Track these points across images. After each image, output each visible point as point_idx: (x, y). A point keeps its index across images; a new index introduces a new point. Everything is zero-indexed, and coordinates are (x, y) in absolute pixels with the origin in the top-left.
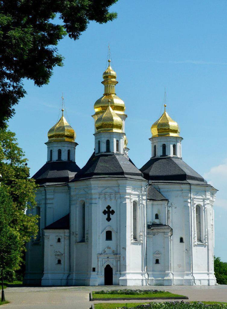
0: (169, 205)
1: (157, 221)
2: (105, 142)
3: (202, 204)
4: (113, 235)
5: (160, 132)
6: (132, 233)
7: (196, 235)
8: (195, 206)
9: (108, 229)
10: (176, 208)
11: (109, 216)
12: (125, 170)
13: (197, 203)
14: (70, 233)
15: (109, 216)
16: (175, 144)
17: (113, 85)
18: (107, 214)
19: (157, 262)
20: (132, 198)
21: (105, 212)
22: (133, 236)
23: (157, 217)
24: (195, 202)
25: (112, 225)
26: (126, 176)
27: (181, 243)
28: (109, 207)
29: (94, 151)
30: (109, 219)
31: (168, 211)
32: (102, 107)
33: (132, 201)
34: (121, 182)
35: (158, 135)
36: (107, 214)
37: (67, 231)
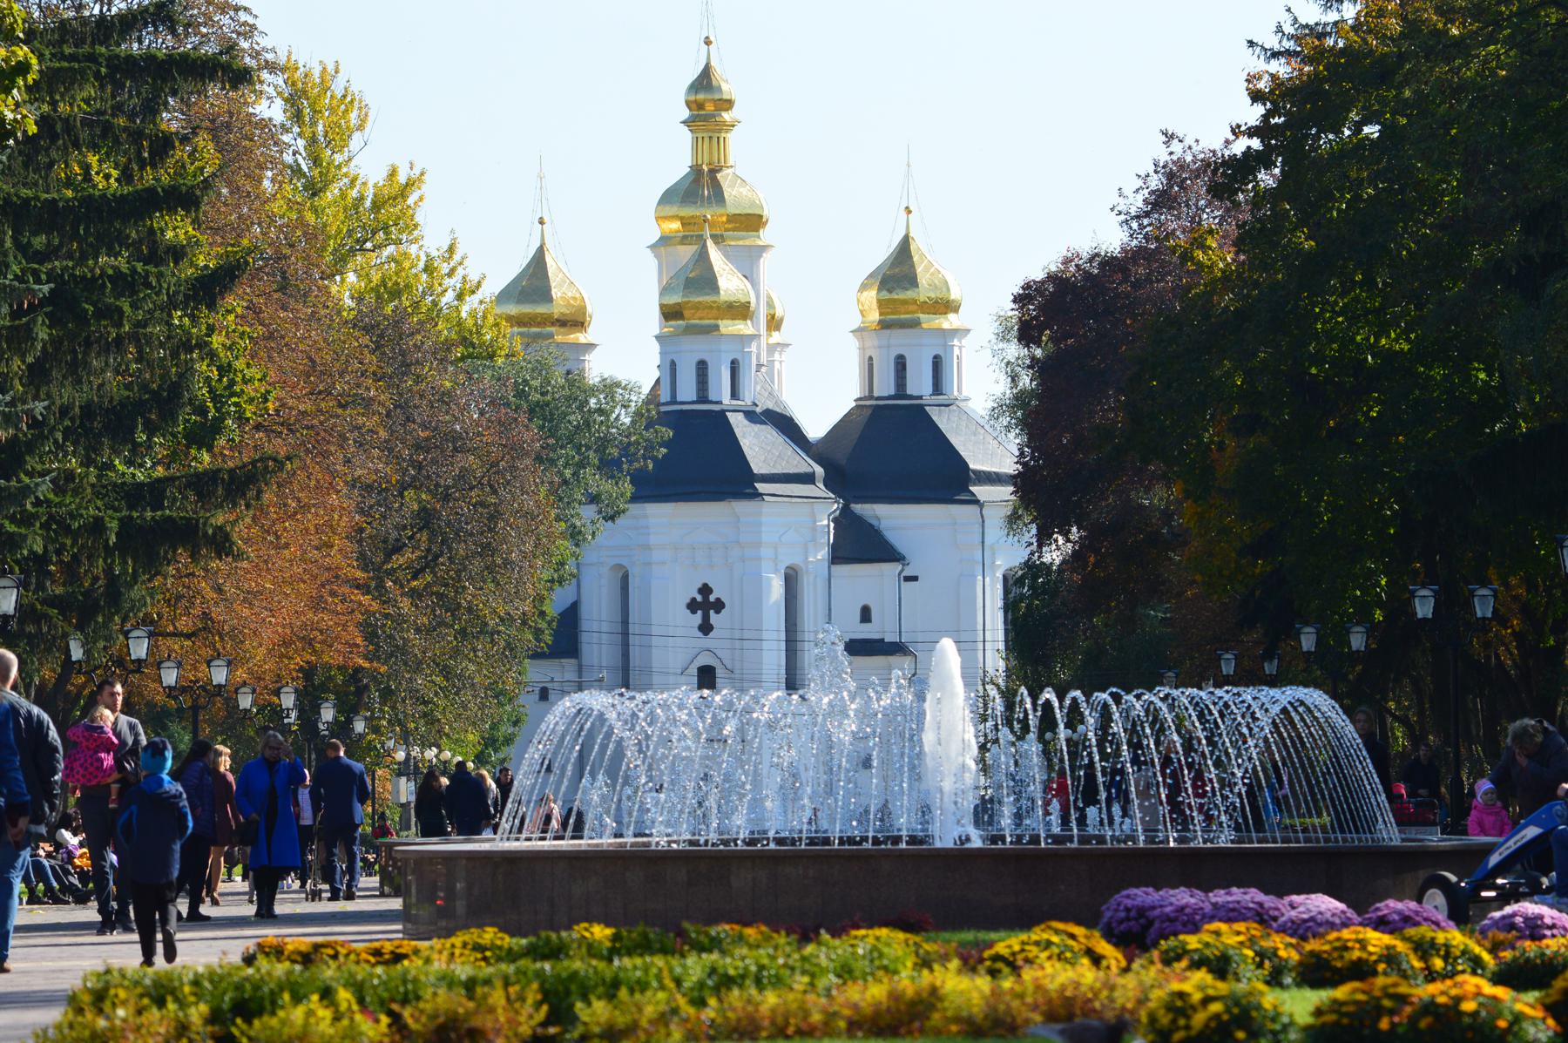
5: (888, 314)
8: (999, 575)
9: (704, 660)
11: (706, 618)
12: (758, 467)
14: (580, 668)
15: (706, 618)
18: (699, 612)
21: (693, 606)
23: (866, 614)
26: (762, 488)
28: (705, 590)
29: (656, 374)
30: (706, 628)
32: (681, 219)
34: (741, 507)
35: (880, 322)
36: (699, 612)
37: (569, 663)
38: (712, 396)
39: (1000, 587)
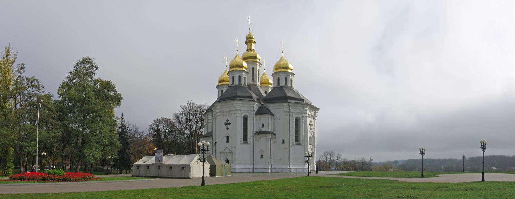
0: (275, 117)
1: (263, 129)
2: (232, 78)
3: (300, 116)
4: (230, 139)
6: (242, 137)
7: (294, 138)
8: (294, 118)
10: (279, 120)
13: (296, 116)
16: (287, 77)
17: (251, 44)
19: (262, 156)
20: (242, 113)
22: (243, 139)
23: (263, 126)
24: (293, 115)
25: (229, 133)
27: (283, 144)
28: (228, 121)
30: (228, 129)
31: (274, 122)
33: (243, 115)
38: (235, 83)
39: (294, 120)
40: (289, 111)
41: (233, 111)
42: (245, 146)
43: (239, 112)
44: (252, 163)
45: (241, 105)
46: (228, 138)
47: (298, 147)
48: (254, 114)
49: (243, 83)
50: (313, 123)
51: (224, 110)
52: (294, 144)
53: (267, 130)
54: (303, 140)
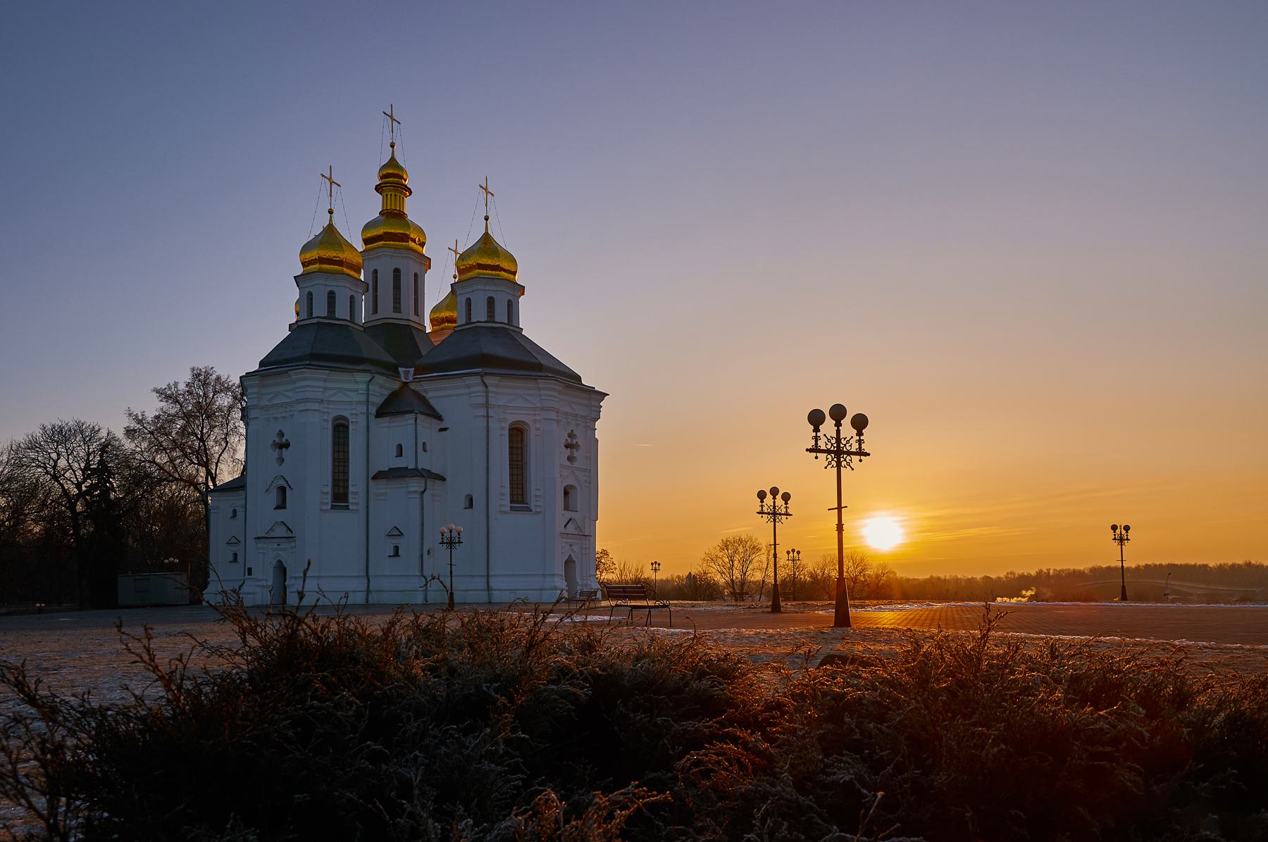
6: (329, 489)
16: (493, 295)
30: (281, 460)
33: (330, 419)
40: (487, 402)
41: (298, 401)
42: (341, 516)
43: (316, 406)
44: (365, 574)
45: (321, 384)
46: (282, 490)
47: (522, 519)
48: (368, 414)
49: (342, 312)
50: (579, 440)
51: (270, 400)
52: (508, 509)
53: (411, 466)
54: (536, 496)
